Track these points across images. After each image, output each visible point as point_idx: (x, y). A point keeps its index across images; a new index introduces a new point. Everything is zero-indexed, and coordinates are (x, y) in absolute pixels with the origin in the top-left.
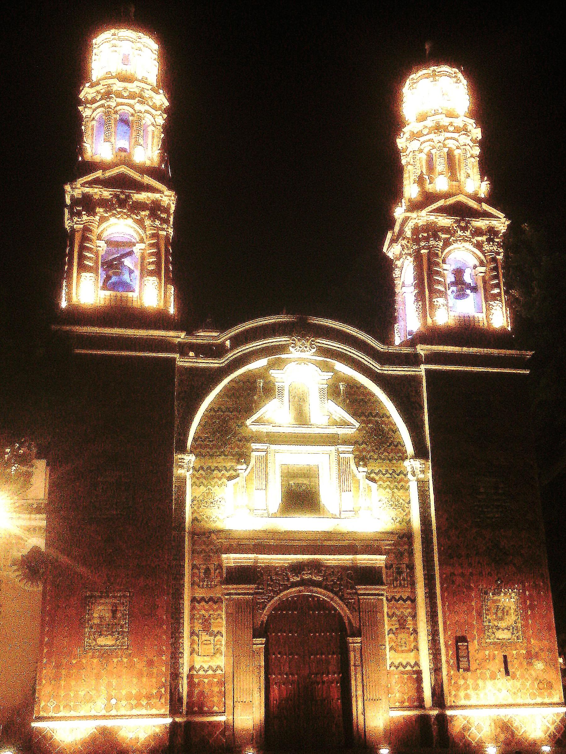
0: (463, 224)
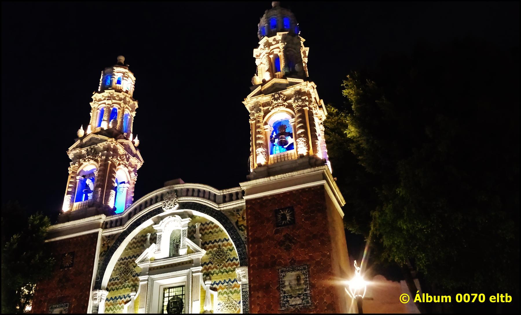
0: (276, 96)
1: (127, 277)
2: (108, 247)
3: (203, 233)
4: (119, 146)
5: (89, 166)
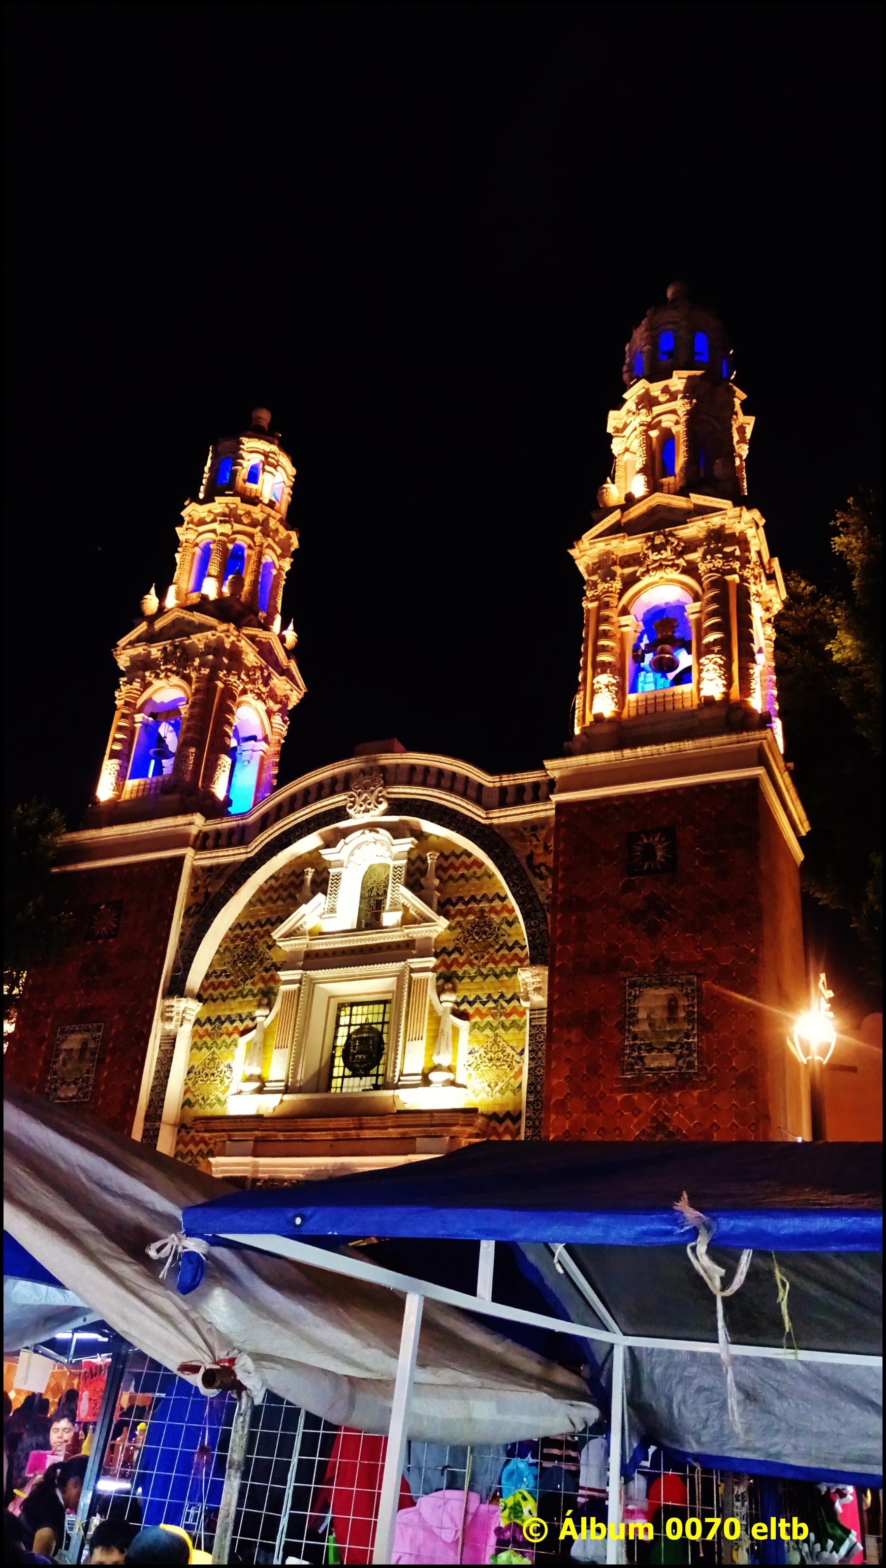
0: (658, 540)
1: (249, 972)
2: (207, 894)
3: (445, 877)
4: (244, 644)
5: (168, 690)
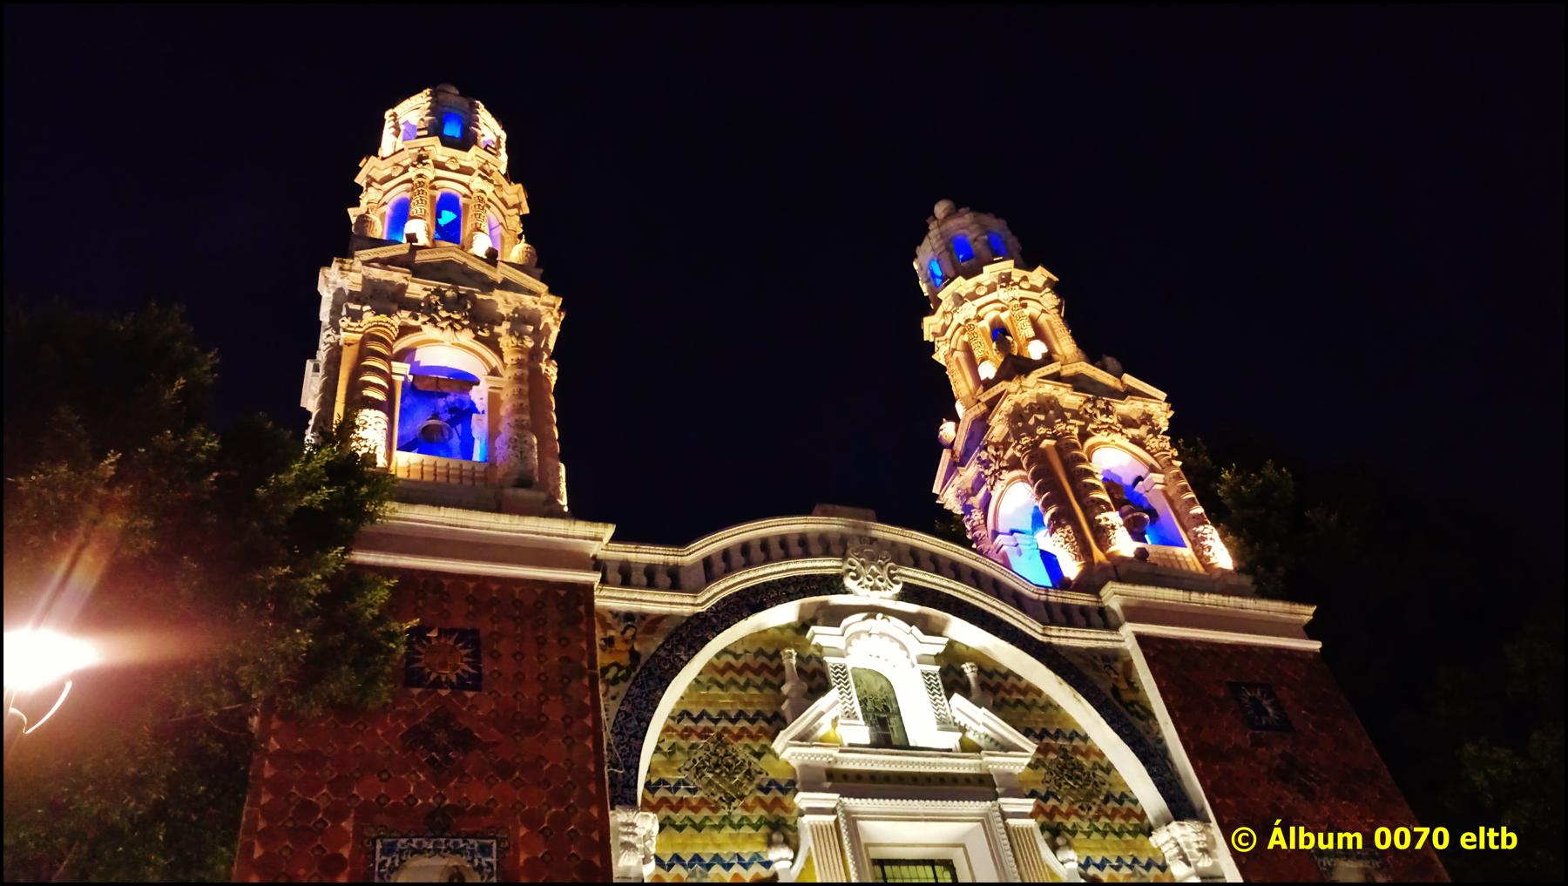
2: (634, 656)
